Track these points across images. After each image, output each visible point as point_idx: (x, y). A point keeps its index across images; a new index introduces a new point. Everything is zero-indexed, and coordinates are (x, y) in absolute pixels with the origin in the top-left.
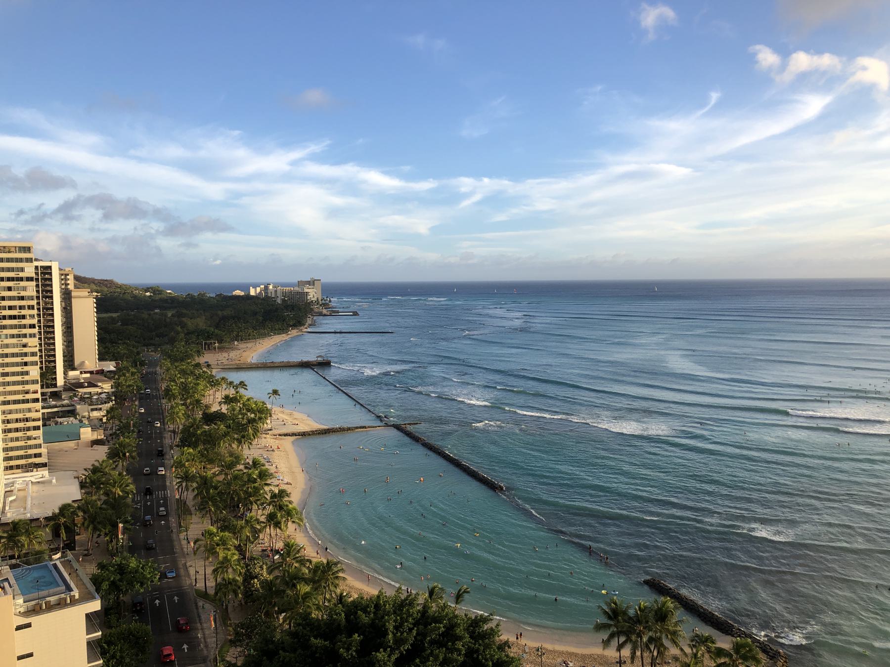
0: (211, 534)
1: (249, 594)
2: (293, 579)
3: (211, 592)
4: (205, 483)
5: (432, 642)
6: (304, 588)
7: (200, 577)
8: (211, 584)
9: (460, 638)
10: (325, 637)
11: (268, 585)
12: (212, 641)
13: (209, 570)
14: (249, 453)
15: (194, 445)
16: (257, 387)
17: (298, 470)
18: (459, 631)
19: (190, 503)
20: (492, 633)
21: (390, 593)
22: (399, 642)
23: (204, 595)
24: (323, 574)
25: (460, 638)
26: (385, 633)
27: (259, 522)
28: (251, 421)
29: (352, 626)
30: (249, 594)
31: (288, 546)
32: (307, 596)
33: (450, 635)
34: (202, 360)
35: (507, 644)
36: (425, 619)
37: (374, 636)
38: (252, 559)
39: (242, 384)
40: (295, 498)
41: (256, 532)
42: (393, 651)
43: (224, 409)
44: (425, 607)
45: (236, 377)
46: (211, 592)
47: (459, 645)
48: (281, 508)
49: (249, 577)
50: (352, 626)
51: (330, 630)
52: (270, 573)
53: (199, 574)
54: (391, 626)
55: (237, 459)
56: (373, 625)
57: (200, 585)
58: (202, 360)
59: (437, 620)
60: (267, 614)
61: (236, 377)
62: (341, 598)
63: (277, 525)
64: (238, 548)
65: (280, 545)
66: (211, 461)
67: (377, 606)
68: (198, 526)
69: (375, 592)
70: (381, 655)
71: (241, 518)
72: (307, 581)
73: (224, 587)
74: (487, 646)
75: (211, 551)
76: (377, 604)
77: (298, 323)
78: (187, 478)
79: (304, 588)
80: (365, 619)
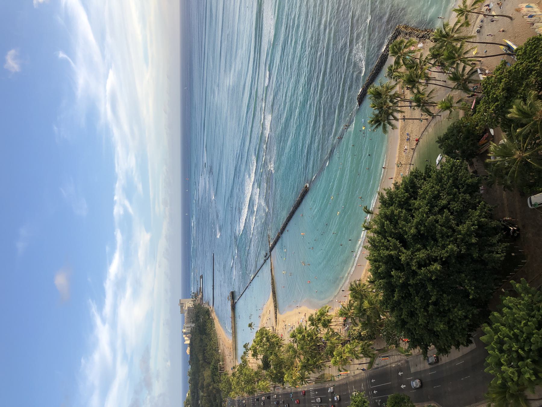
0: (335, 363)
1: (371, 337)
2: (361, 311)
3: (369, 360)
4: (305, 367)
5: (395, 228)
6: (366, 304)
7: (361, 367)
8: (364, 360)
9: (392, 212)
10: (393, 291)
11: (365, 326)
12: (396, 358)
13: (356, 361)
14: (287, 340)
15: (283, 374)
16: (248, 337)
17: (297, 310)
18: (388, 212)
19: (317, 375)
20: (389, 193)
21: (367, 253)
22: (395, 248)
23: (371, 364)
24: (357, 292)
25: (392, 212)
26: (390, 256)
27: (328, 333)
28: (268, 340)
29: (387, 275)
30: (371, 337)
31: (341, 315)
32: (370, 303)
33: (390, 218)
34: (230, 372)
35: (395, 184)
36: (382, 232)
37: (393, 262)
38: (349, 336)
39: (245, 346)
40: (313, 312)
41: (334, 334)
42: (400, 251)
43: (260, 357)
44: (375, 232)
45: (241, 350)
46: (369, 360)
47: (396, 212)
48: (319, 319)
49: (360, 338)
50: (387, 275)
51: (390, 289)
52: (357, 325)
53: (357, 368)
54: (386, 253)
55: (291, 347)
56: (386, 263)
57: (365, 367)
58: (230, 372)
59: (382, 225)
60: (381, 325)
61: (241, 350)
62: (371, 282)
63: (329, 321)
64: (343, 344)
65: (341, 319)
66: (292, 363)
67: (375, 261)
68: (331, 370)
69: (368, 262)
70: (403, 258)
71: (325, 343)
72: (362, 303)
73: (365, 353)
74: (397, 195)
75: (345, 362)
76: (374, 261)
77: (208, 313)
78: (302, 378)
79: (366, 304)
80: (382, 268)
